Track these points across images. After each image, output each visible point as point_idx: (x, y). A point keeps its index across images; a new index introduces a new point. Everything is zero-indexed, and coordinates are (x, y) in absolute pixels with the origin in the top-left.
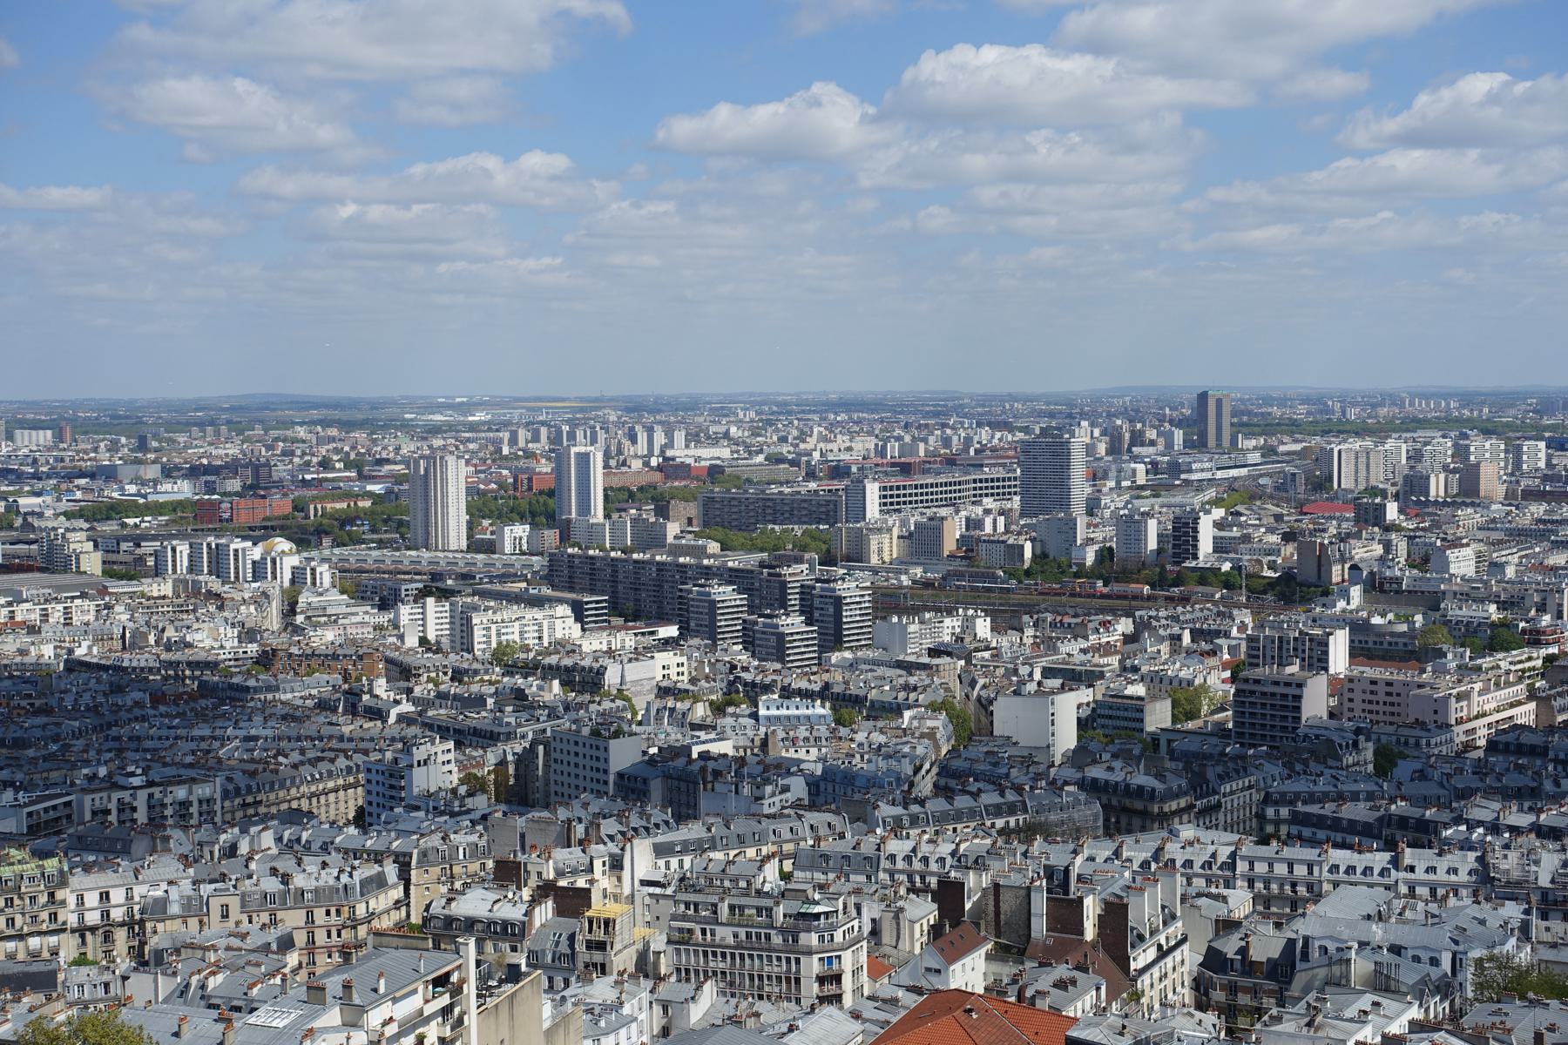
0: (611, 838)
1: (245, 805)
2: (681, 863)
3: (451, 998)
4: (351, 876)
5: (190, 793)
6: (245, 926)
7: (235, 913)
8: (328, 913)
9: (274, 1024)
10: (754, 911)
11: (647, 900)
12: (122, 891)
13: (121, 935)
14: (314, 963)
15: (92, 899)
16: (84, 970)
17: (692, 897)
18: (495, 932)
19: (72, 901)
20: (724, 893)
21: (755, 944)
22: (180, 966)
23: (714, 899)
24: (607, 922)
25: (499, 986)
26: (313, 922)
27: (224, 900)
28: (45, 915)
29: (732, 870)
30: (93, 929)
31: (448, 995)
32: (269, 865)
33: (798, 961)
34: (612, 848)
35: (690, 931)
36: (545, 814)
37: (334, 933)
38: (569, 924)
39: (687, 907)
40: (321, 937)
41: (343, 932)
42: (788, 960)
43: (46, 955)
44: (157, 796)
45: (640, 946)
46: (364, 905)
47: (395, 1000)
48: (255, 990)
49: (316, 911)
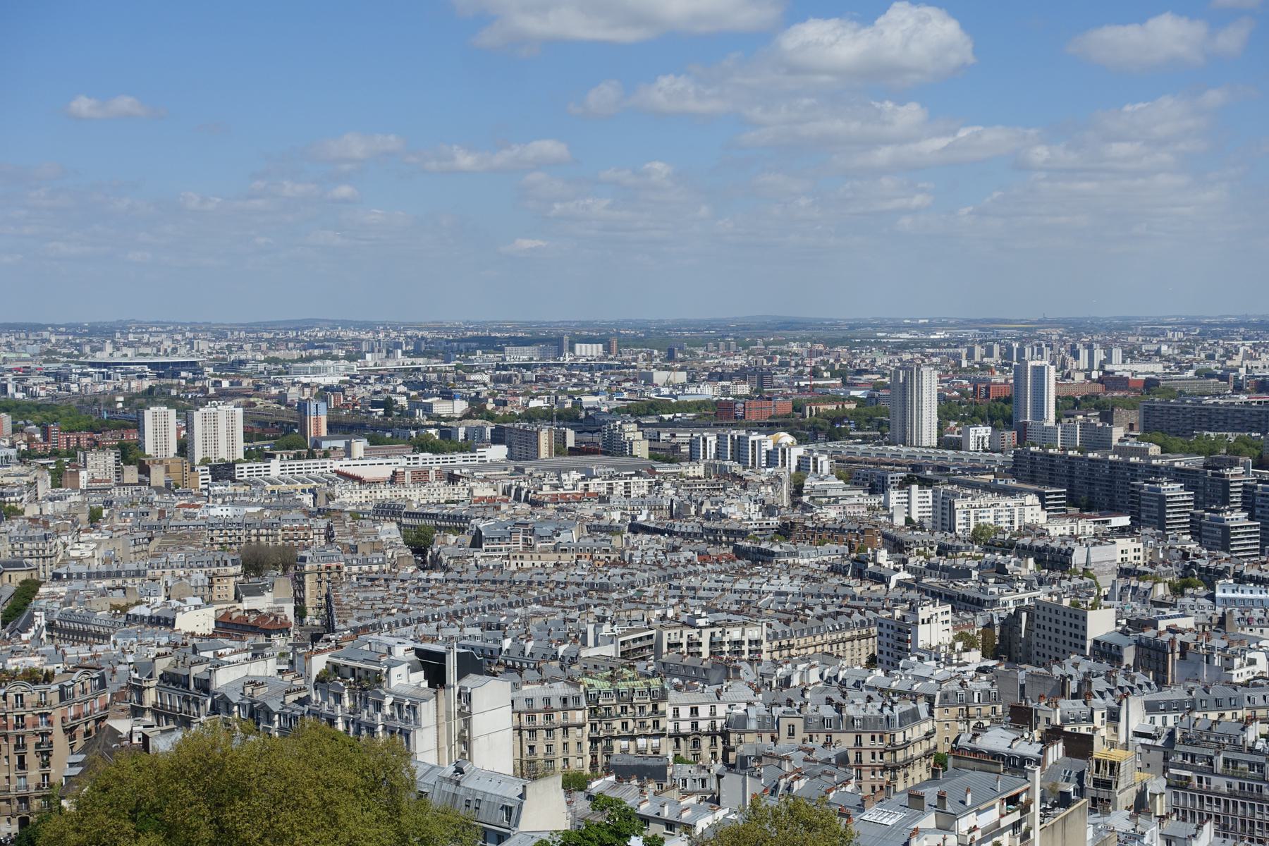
0: (1101, 694)
1: (780, 648)
3: (1021, 815)
4: (892, 709)
5: (743, 634)
6: (809, 745)
7: (800, 734)
8: (873, 738)
9: (884, 822)
10: (1247, 766)
11: (1139, 749)
13: (706, 742)
14: (861, 778)
15: (685, 712)
16: (687, 767)
17: (1190, 749)
18: (1014, 766)
19: (670, 712)
20: (1219, 747)
22: (762, 771)
23: (1211, 752)
24: (1112, 765)
25: (1052, 809)
26: (861, 744)
27: (791, 721)
28: (650, 722)
29: (1218, 729)
30: (685, 736)
31: (1019, 812)
32: (825, 696)
34: (1110, 701)
35: (1187, 778)
36: (1042, 670)
37: (878, 755)
38: (1079, 764)
39: (1185, 756)
40: (867, 757)
41: (885, 755)
43: (650, 752)
44: (718, 635)
45: (1139, 788)
46: (902, 734)
47: (979, 812)
48: (831, 795)
49: (863, 736)
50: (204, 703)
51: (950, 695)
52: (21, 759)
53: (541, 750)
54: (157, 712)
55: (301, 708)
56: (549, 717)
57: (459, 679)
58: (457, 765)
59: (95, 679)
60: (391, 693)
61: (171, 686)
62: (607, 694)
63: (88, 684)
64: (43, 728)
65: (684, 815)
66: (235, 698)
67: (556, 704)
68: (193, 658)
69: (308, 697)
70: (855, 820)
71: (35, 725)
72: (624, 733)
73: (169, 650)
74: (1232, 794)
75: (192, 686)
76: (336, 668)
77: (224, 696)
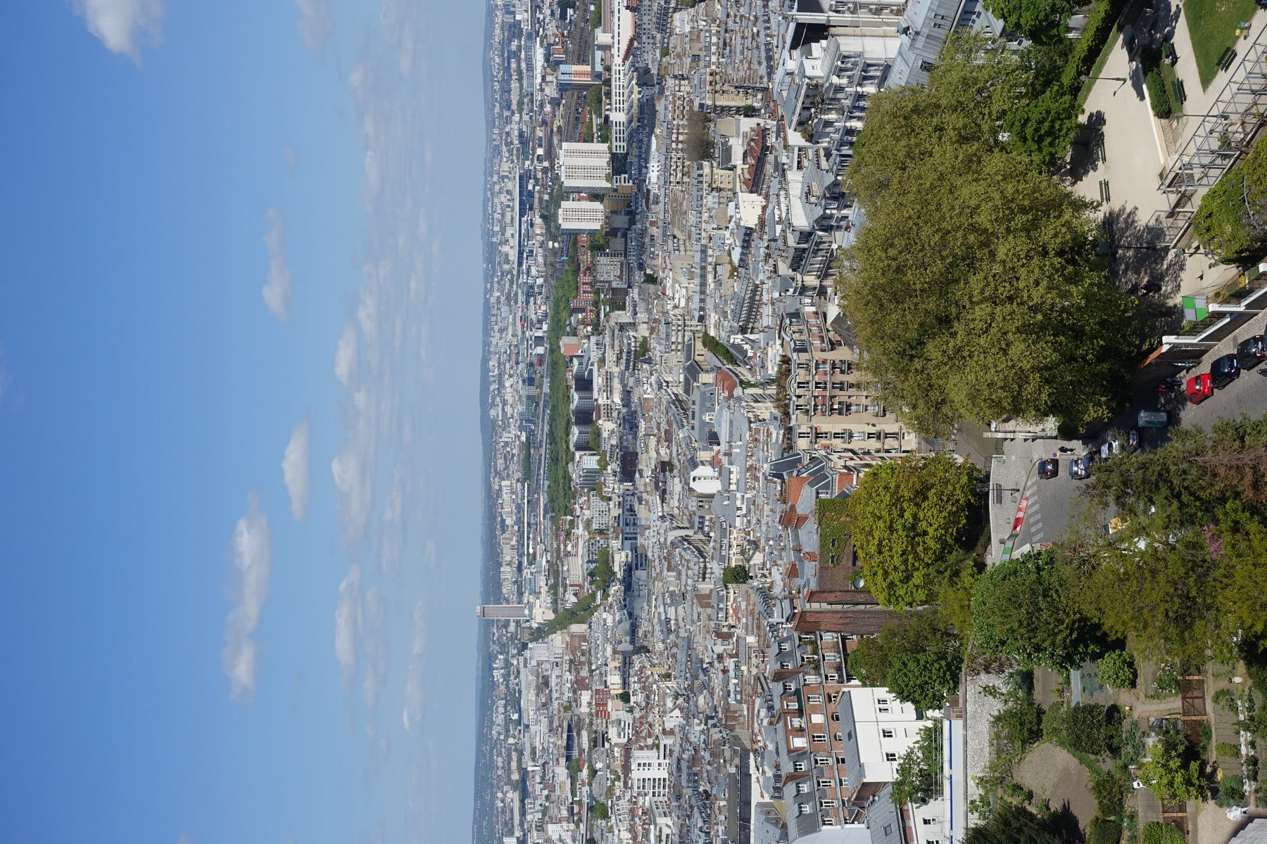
50: (820, 237)
54: (824, 275)
55: (833, 156)
57: (821, 11)
58: (901, 31)
59: (791, 322)
60: (828, 77)
61: (803, 263)
63: (794, 328)
64: (828, 367)
68: (780, 243)
69: (825, 149)
71: (825, 373)
73: (771, 261)
75: (805, 246)
76: (801, 123)
77: (817, 221)
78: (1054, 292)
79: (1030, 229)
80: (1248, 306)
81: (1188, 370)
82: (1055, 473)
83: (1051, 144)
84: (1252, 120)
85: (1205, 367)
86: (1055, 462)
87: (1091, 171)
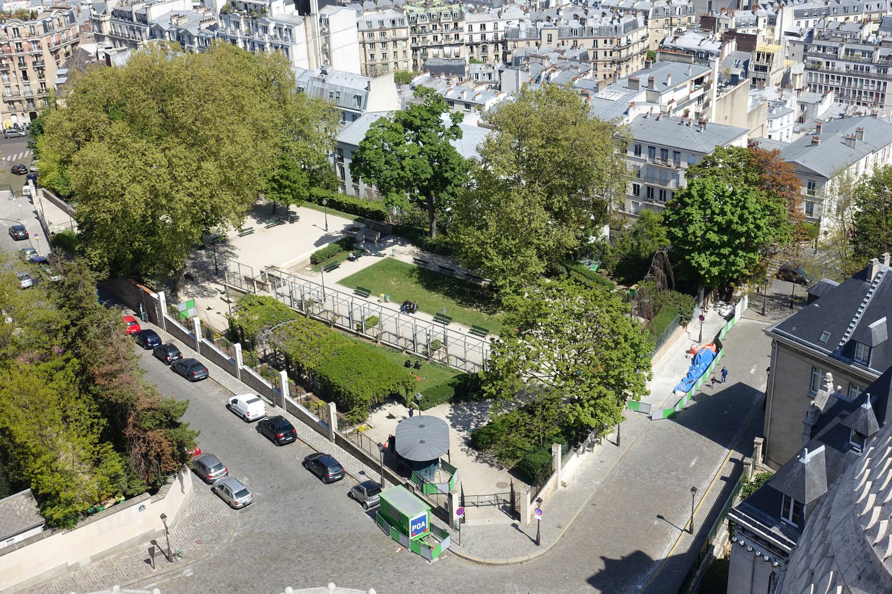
2: (807, 22)
3: (704, 91)
4: (619, 21)
6: (562, 48)
7: (556, 40)
8: (605, 42)
9: (611, 99)
10: (861, 53)
11: (788, 44)
12: (492, 24)
13: (491, 48)
14: (596, 70)
15: (476, 28)
16: (479, 66)
17: (822, 43)
18: (701, 58)
20: (843, 41)
21: (860, 73)
22: (530, 66)
23: (837, 45)
25: (725, 87)
26: (597, 46)
27: (550, 32)
28: (452, 35)
29: (843, 28)
30: (477, 45)
31: (703, 89)
32: (573, 13)
33: (885, 84)
35: (819, 63)
37: (608, 54)
38: (745, 55)
39: (819, 48)
40: (601, 55)
41: (613, 53)
42: (879, 83)
43: (453, 57)
45: (785, 70)
46: (625, 38)
47: (675, 90)
48: (576, 82)
49: (599, 40)
50: (145, 30)
51: (659, 10)
52: (24, 73)
53: (379, 57)
55: (212, 32)
56: (383, 34)
57: (320, 8)
58: (323, 69)
59: (67, 16)
60: (273, 20)
61: (120, 19)
62: (422, 17)
63: (62, 20)
64: (36, 51)
65: (477, 98)
66: (166, 27)
67: (388, 24)
70: (592, 98)
71: (30, 50)
72: (435, 43)
74: (848, 73)
75: (135, 19)
77: (157, 26)
78: (185, 208)
79: (227, 183)
80: (202, 344)
81: (139, 315)
82: (17, 239)
83: (273, 189)
84: (330, 317)
85: (144, 326)
86: (26, 237)
87: (256, 221)
